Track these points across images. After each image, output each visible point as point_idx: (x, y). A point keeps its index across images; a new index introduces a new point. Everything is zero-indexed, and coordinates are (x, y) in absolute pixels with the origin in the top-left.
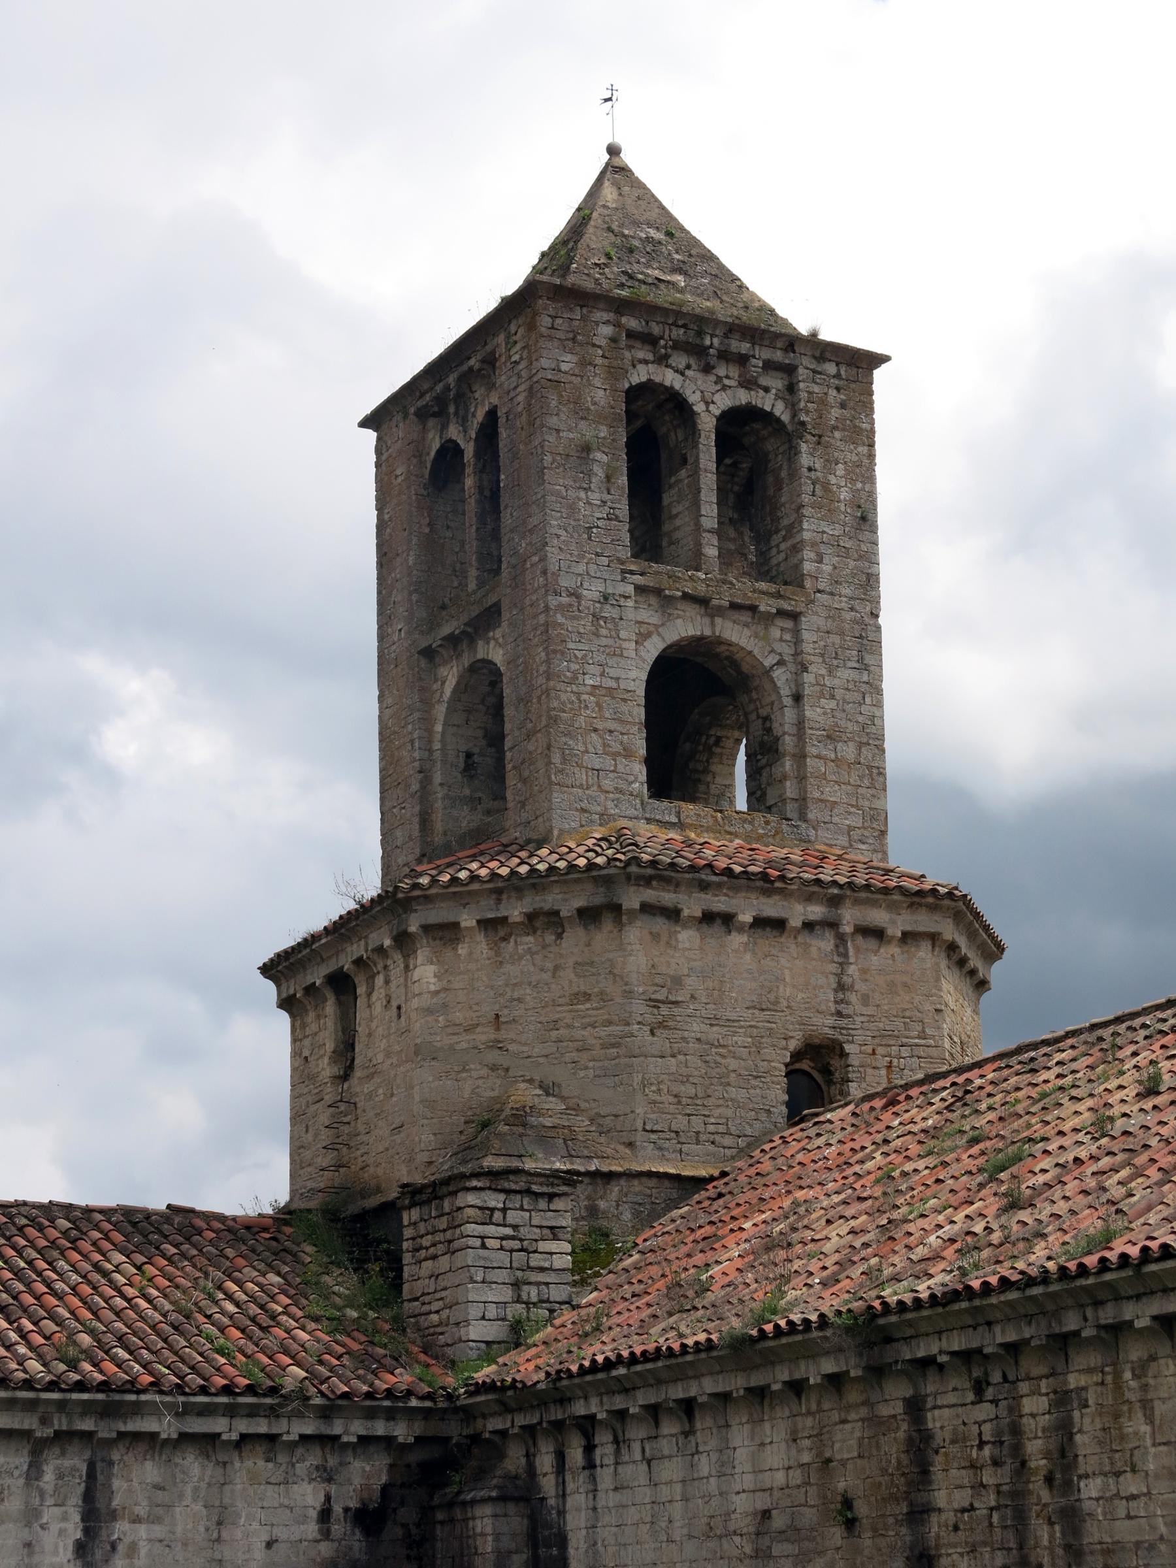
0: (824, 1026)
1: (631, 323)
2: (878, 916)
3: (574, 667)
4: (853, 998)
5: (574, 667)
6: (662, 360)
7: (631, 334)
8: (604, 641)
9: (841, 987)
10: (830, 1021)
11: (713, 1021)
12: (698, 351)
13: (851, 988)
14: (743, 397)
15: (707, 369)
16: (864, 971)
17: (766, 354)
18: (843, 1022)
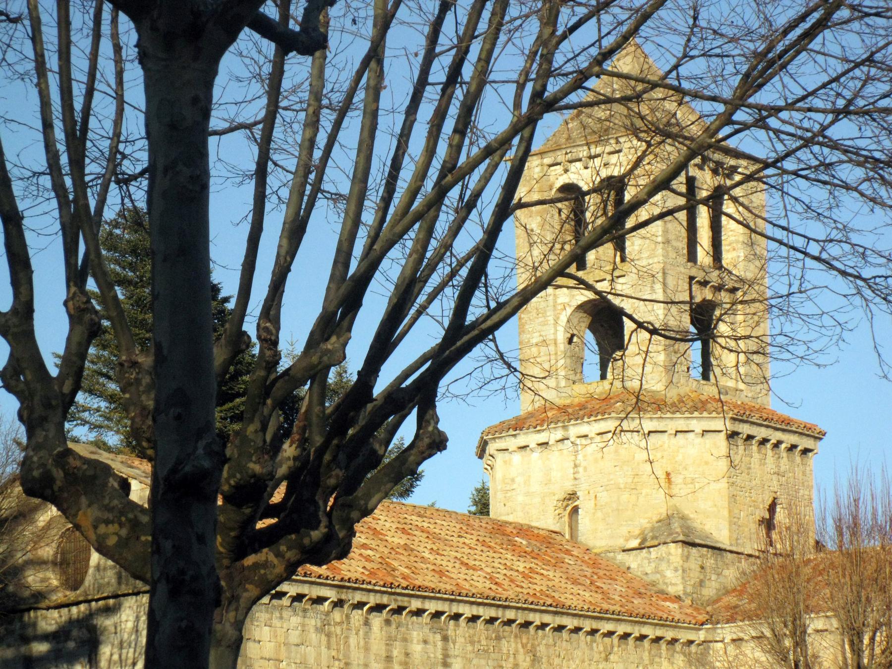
0: (569, 487)
1: (548, 160)
2: (584, 429)
3: (528, 336)
4: (581, 469)
5: (528, 336)
6: (566, 171)
7: (550, 166)
8: (541, 320)
9: (576, 466)
10: (571, 483)
11: (527, 494)
12: (580, 160)
13: (579, 466)
14: (604, 173)
15: (586, 168)
16: (585, 456)
17: (608, 149)
18: (577, 482)
